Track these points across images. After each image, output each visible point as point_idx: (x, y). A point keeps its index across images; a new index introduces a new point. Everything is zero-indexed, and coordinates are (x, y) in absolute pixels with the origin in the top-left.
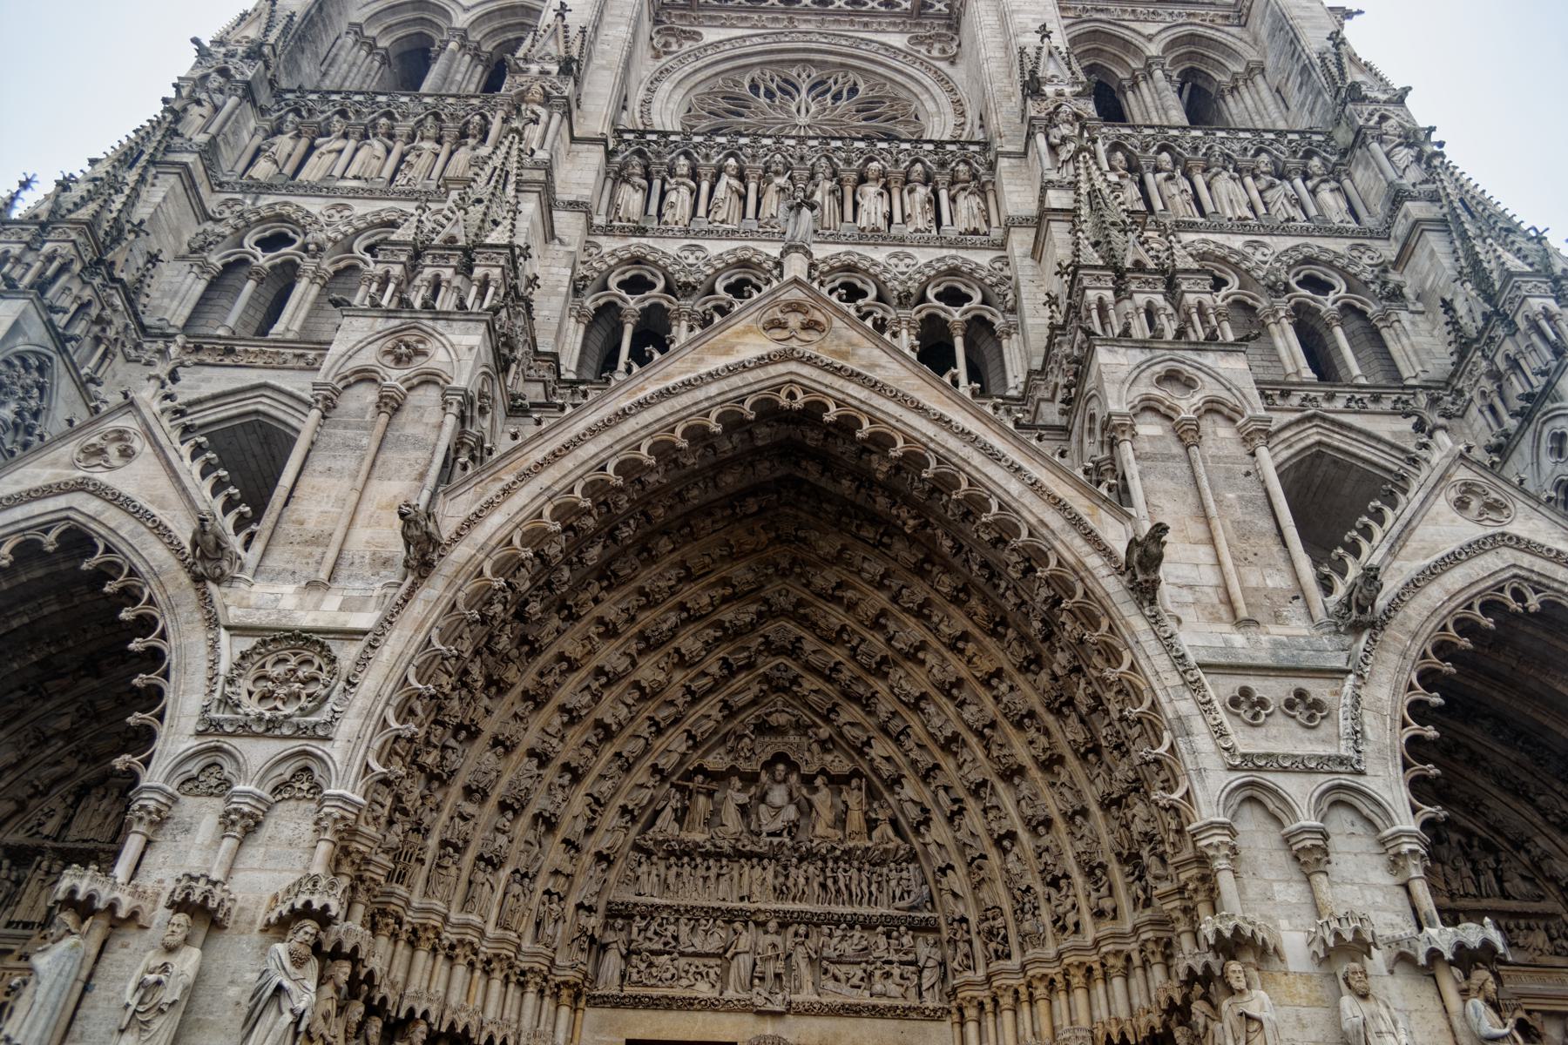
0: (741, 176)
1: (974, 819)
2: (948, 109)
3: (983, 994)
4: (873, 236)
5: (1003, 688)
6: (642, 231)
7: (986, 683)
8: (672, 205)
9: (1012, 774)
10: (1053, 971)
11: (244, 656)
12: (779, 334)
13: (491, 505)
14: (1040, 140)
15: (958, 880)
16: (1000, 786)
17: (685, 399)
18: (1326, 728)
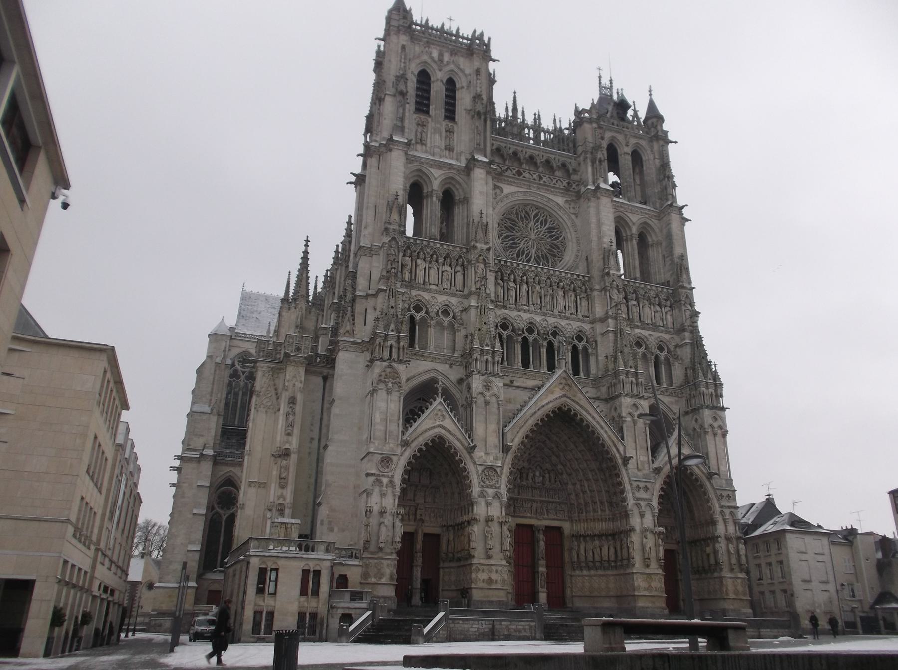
0: (527, 283)
1: (578, 486)
2: (574, 240)
3: (577, 519)
4: (562, 315)
5: (589, 462)
6: (505, 307)
7: (586, 461)
8: (512, 296)
9: (588, 480)
10: (592, 518)
11: (483, 471)
12: (561, 387)
13: (516, 436)
14: (608, 293)
15: (573, 496)
16: (585, 481)
17: (545, 408)
18: (648, 492)
